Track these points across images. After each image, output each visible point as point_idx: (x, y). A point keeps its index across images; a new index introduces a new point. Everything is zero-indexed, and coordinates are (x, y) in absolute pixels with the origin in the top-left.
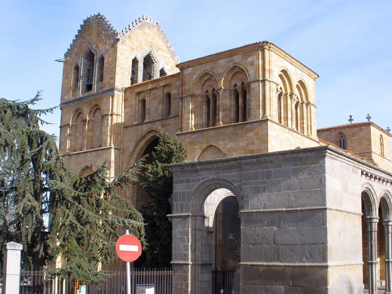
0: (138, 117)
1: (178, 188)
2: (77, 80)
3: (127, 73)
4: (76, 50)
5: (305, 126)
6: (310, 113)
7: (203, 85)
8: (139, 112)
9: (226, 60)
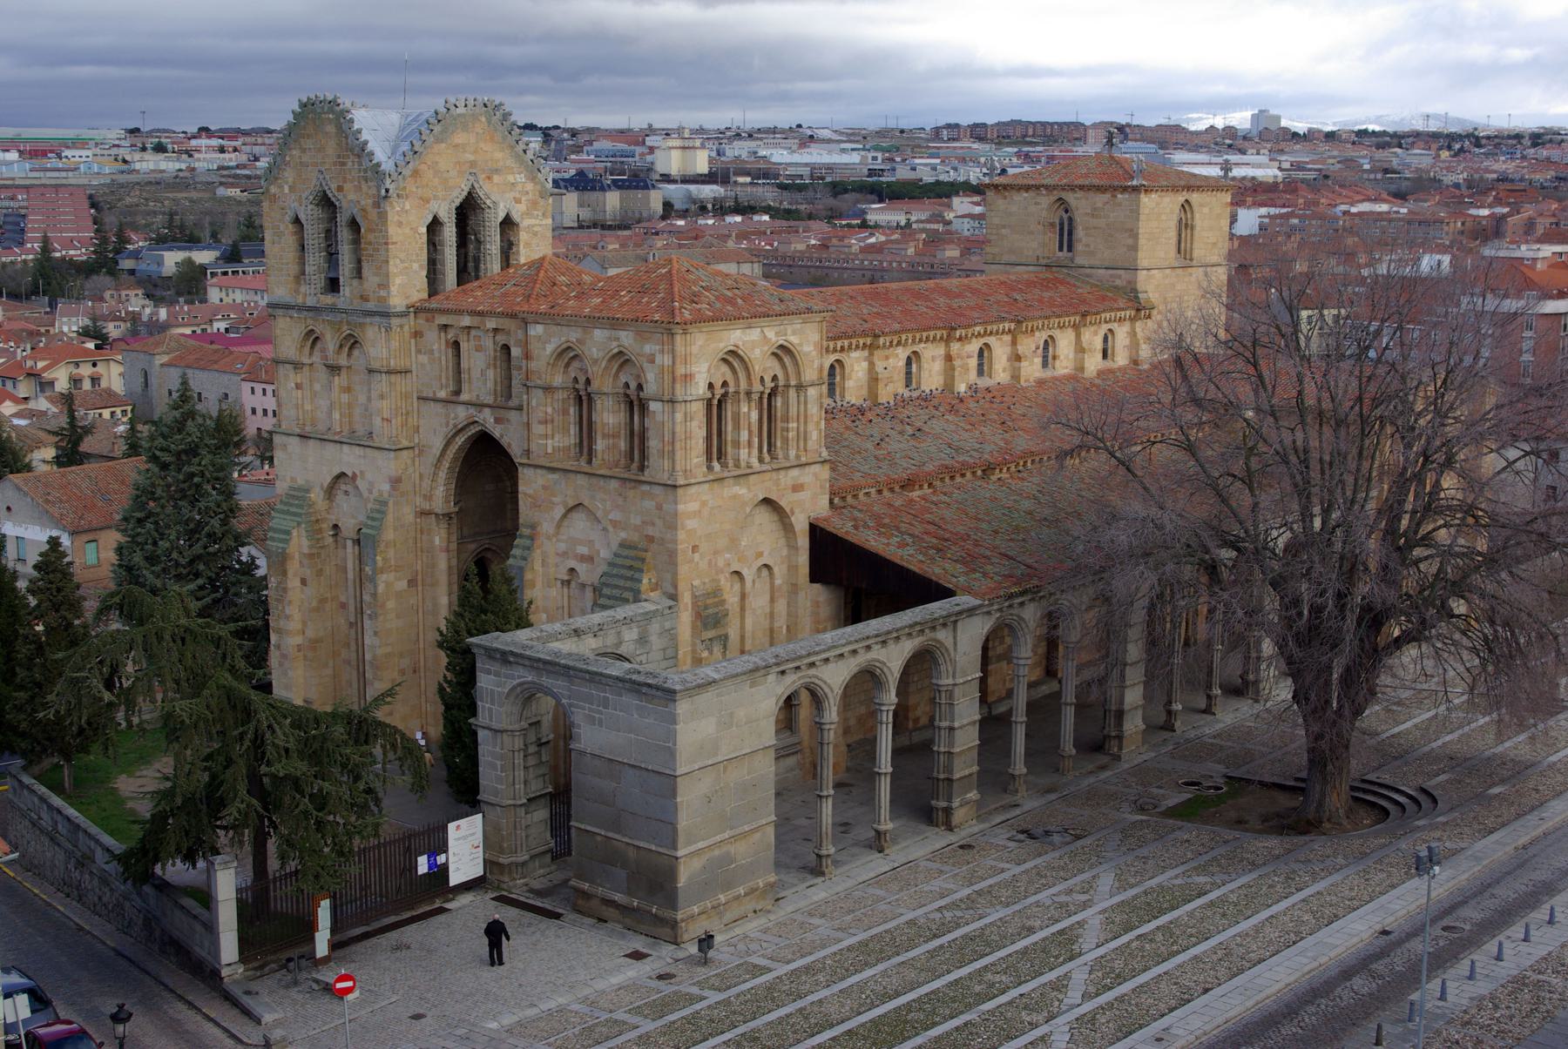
0: (447, 379)
1: (485, 681)
3: (415, 266)
6: (806, 403)
7: (567, 365)
8: (447, 368)
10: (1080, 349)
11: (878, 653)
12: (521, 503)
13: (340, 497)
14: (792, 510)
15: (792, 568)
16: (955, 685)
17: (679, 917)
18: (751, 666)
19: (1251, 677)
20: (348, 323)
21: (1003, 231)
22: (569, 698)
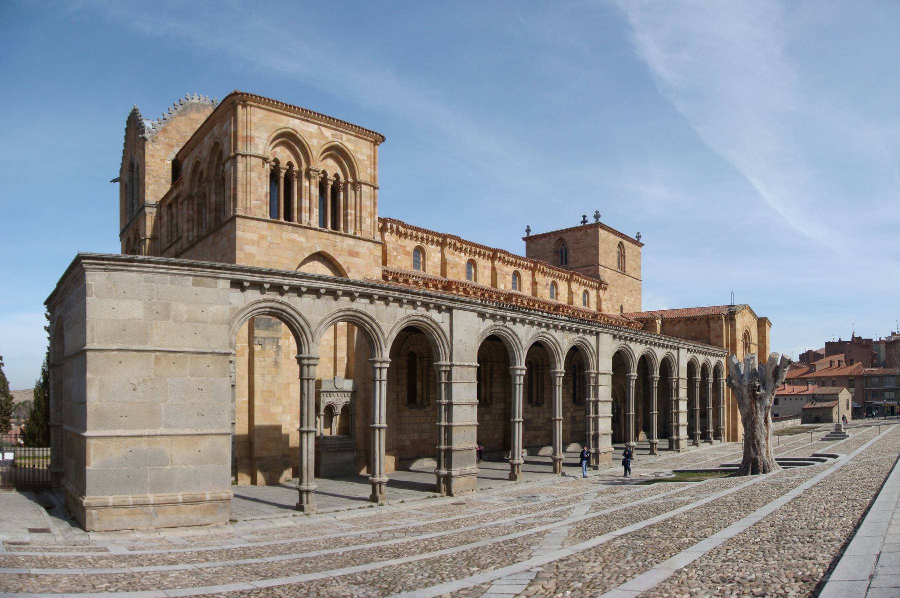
5: (351, 218)
14: (348, 268)
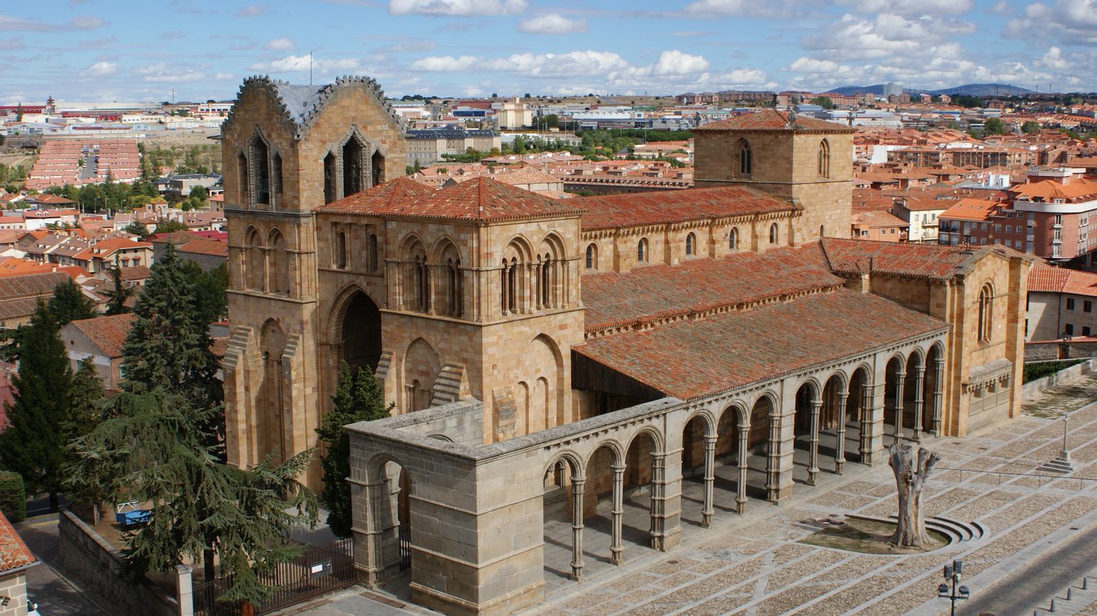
1: (354, 453)
2: (245, 173)
3: (317, 184)
4: (237, 127)
5: (559, 292)
7: (412, 248)
9: (437, 227)
10: (755, 236)
11: (612, 435)
12: (383, 337)
13: (269, 334)
15: (560, 379)
16: (665, 456)
17: (479, 608)
18: (526, 443)
19: (866, 450)
20: (274, 222)
21: (706, 160)
22: (408, 464)
